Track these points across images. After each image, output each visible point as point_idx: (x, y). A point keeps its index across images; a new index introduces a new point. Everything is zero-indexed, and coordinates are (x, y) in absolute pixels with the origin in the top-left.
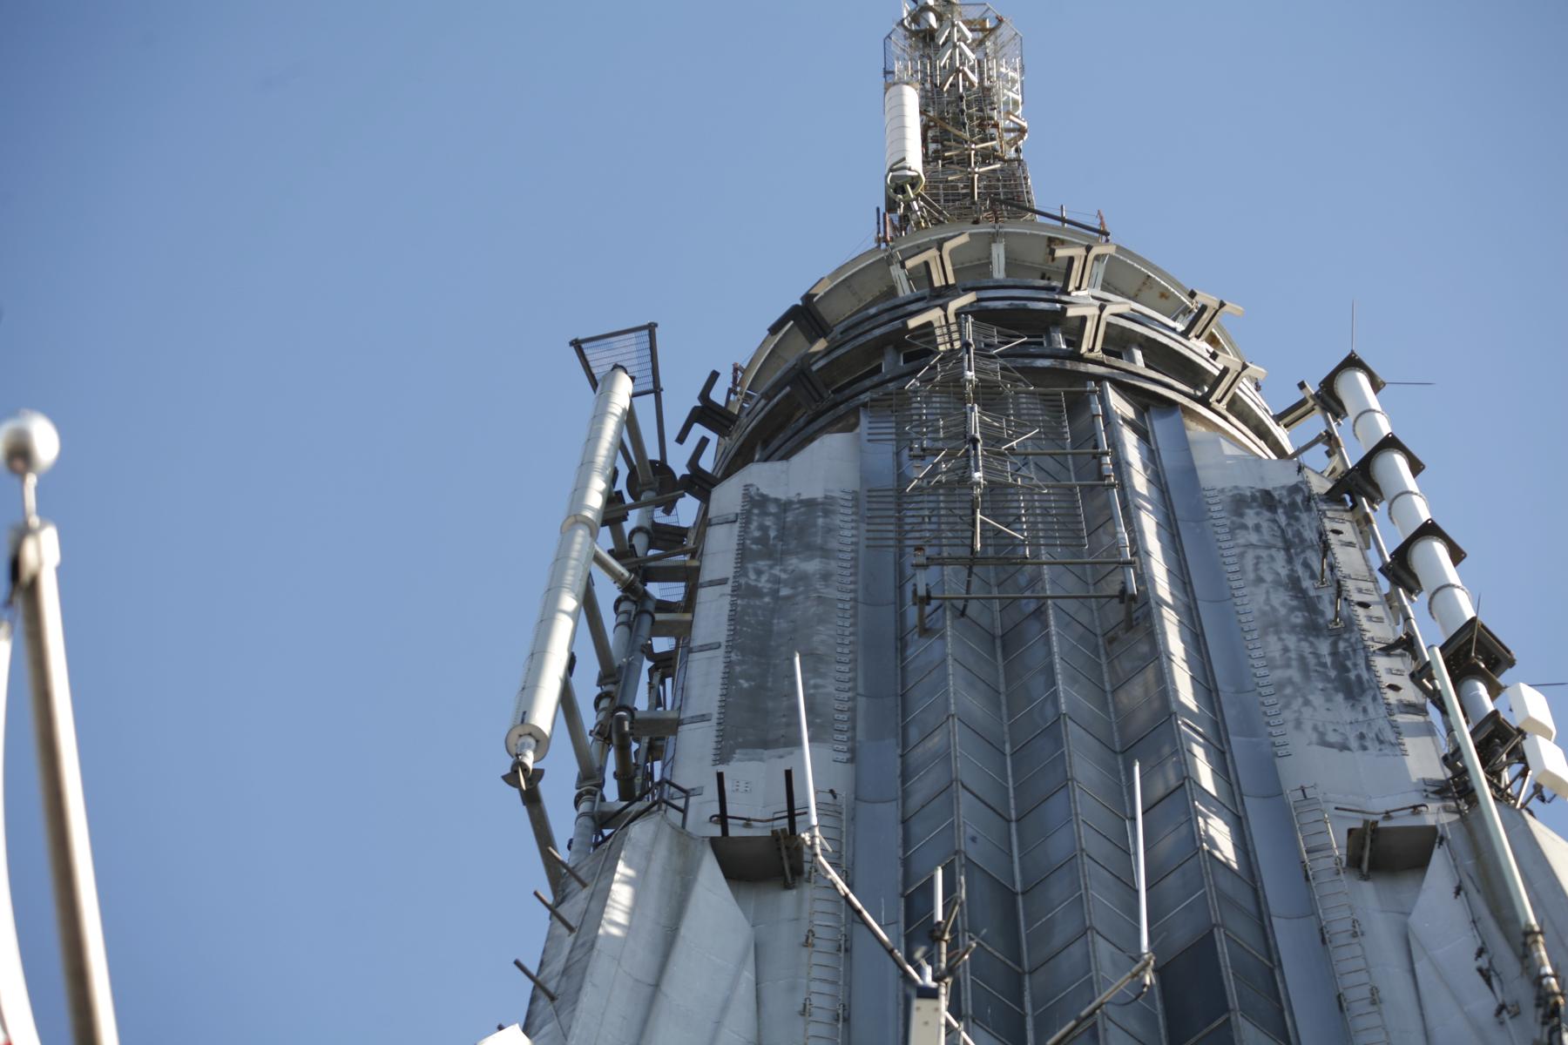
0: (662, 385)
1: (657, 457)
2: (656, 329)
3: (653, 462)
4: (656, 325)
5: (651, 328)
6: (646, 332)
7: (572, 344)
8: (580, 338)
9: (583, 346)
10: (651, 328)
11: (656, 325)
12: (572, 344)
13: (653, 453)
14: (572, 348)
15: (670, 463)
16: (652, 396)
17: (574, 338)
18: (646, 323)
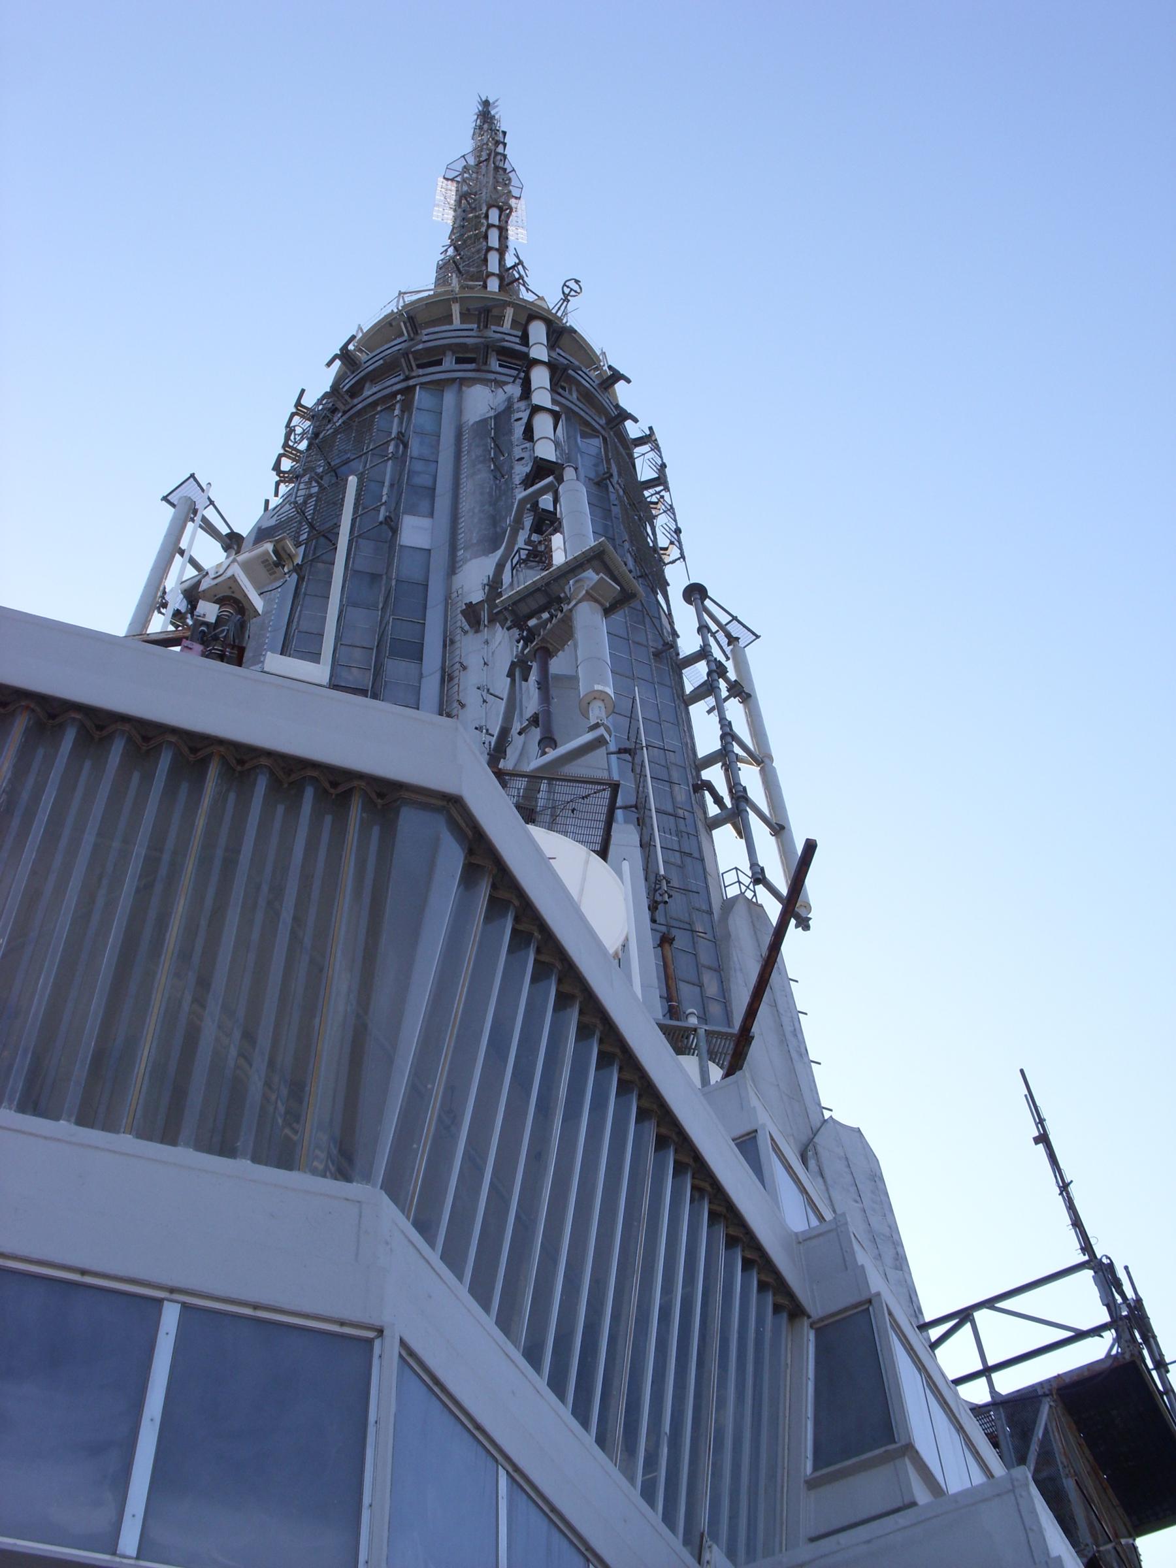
0: (213, 499)
1: (229, 531)
2: (195, 476)
3: (227, 535)
4: (194, 474)
5: (192, 476)
6: (192, 479)
7: (162, 500)
8: (165, 495)
9: (169, 498)
10: (192, 476)
11: (194, 474)
12: (162, 500)
13: (225, 531)
14: (163, 502)
15: (235, 531)
16: (211, 506)
17: (162, 497)
18: (189, 475)
